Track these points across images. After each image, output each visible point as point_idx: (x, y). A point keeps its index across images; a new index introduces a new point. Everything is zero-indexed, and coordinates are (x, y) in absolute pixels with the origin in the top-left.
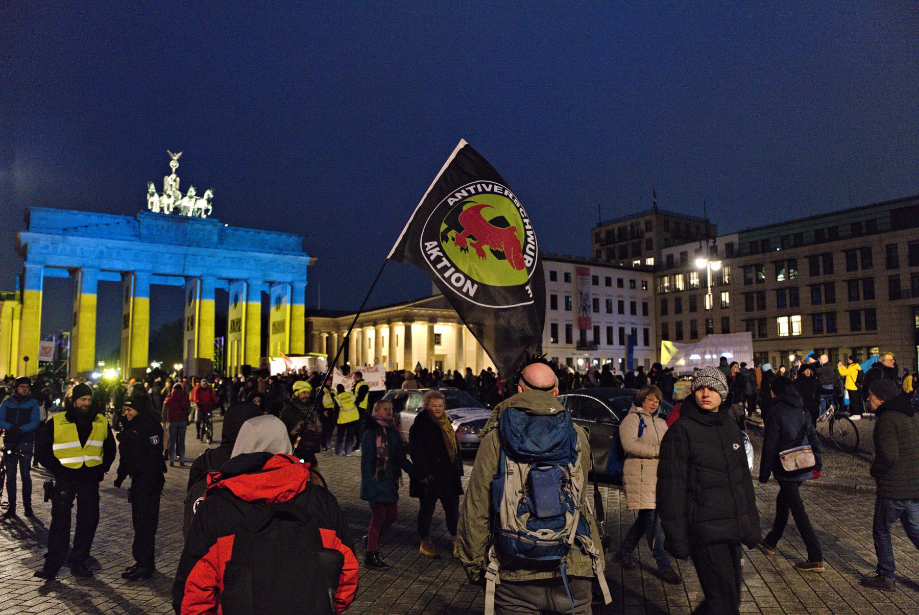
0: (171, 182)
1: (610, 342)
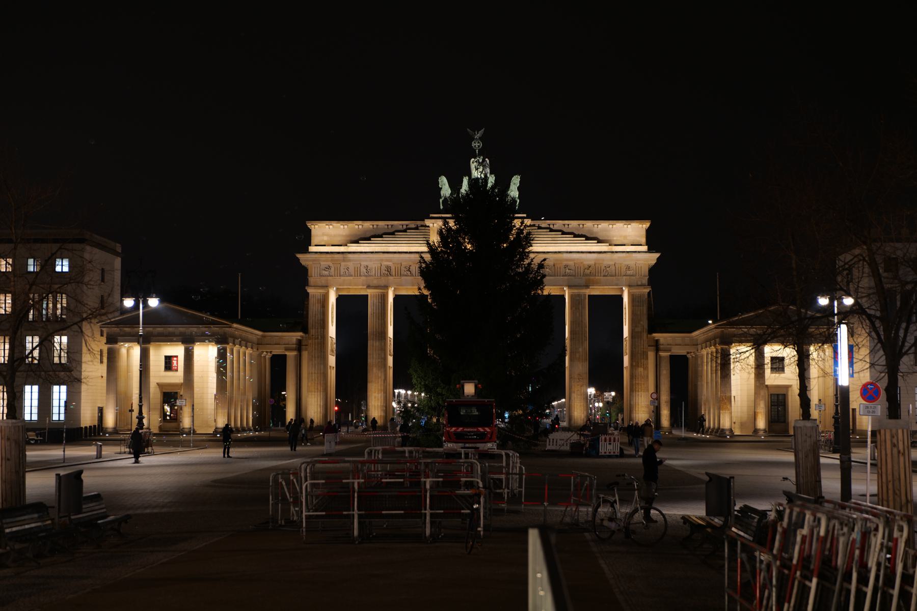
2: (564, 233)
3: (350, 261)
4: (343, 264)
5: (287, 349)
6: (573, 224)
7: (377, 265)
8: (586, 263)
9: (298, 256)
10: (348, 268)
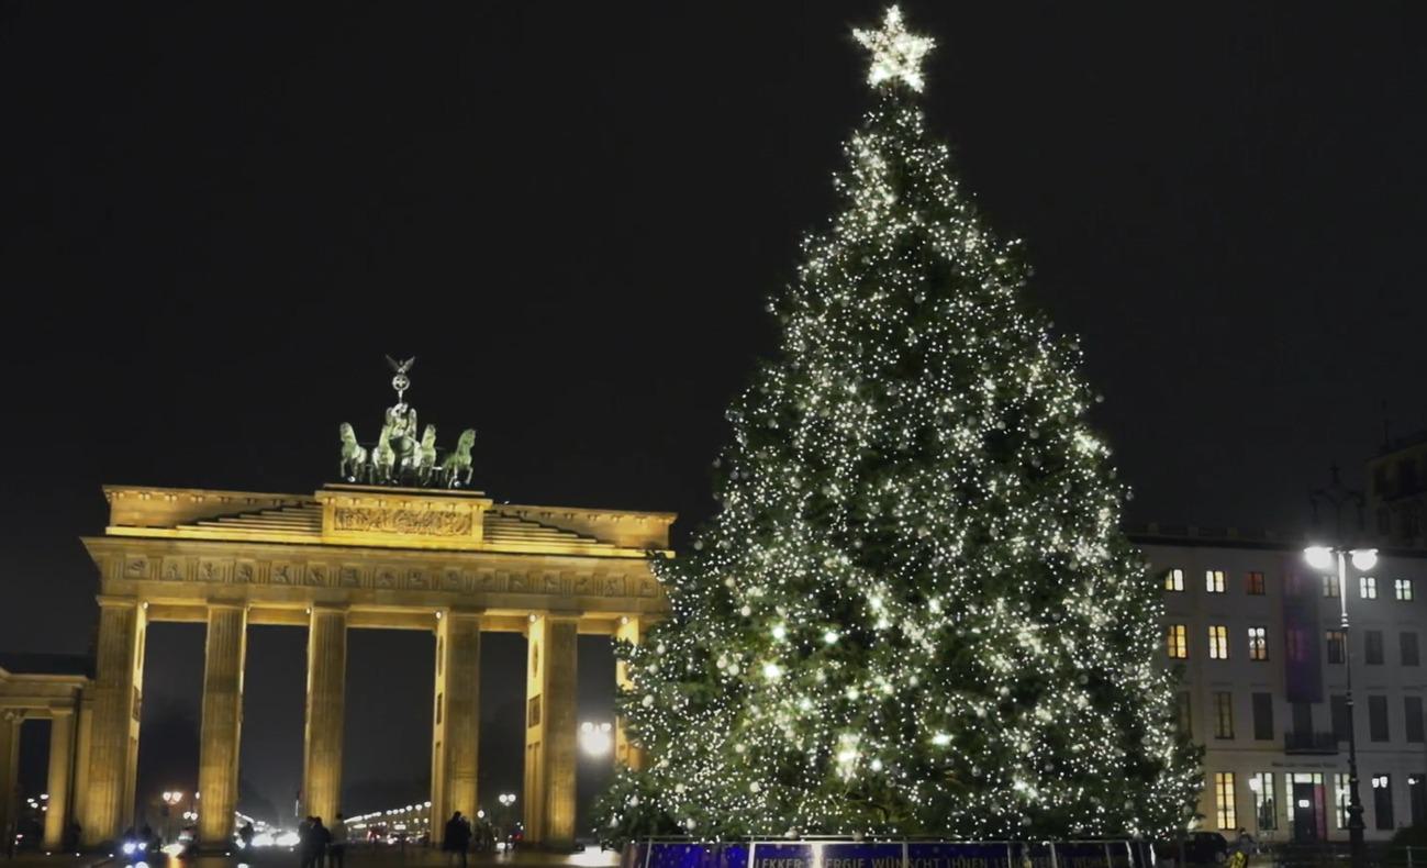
0: (398, 421)
1: (1380, 732)
2: (542, 526)
3: (179, 553)
4: (167, 558)
5: (55, 705)
6: (558, 512)
7: (228, 564)
8: (581, 574)
9: (87, 541)
10: (175, 568)
